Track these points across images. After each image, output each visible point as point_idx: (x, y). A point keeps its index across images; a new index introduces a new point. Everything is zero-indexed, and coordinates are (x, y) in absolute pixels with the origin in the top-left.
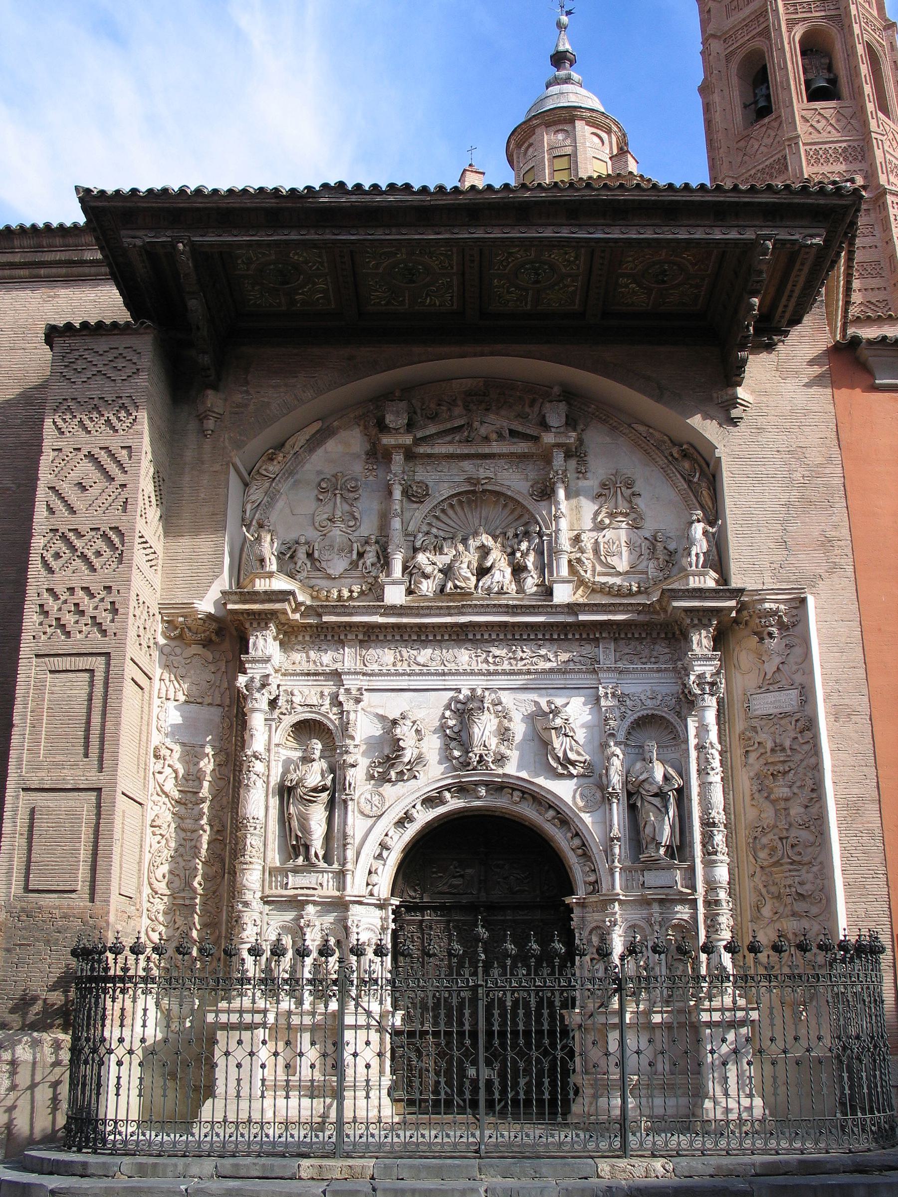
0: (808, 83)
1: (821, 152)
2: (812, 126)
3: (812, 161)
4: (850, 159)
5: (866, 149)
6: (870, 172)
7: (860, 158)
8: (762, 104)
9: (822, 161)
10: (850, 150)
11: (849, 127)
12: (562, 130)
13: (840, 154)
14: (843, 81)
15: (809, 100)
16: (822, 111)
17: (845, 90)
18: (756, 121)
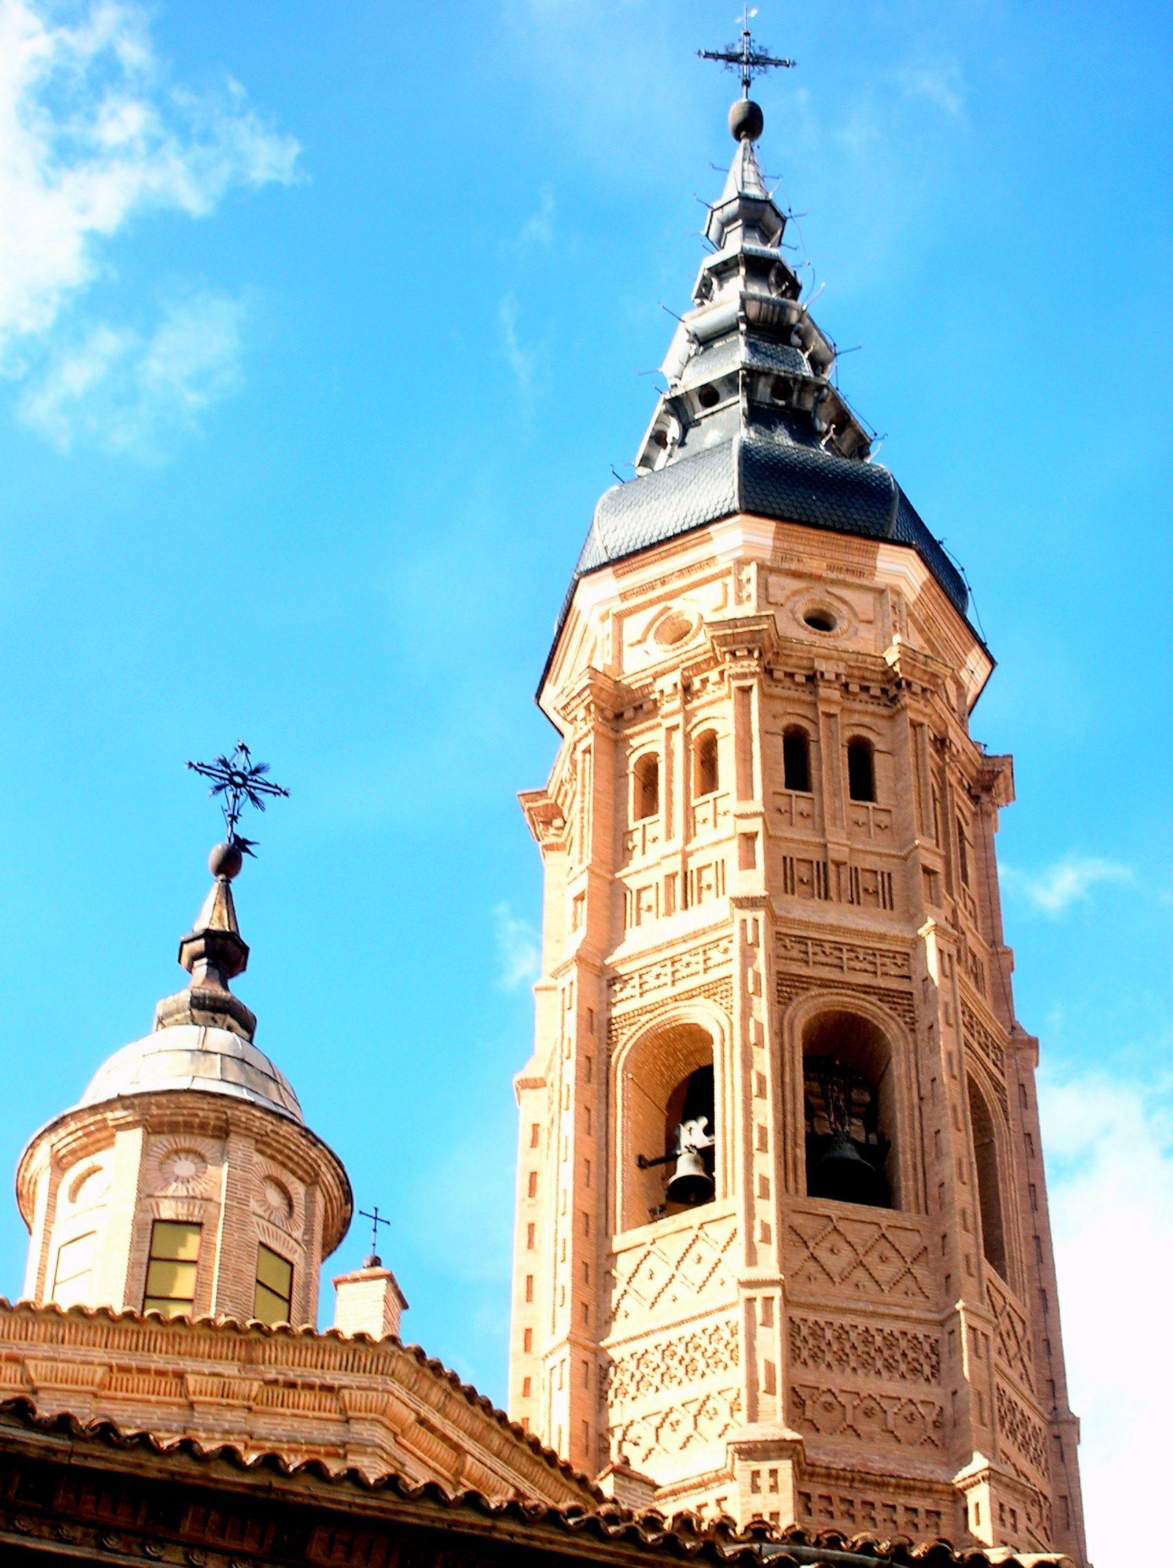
0: (815, 1144)
1: (829, 1334)
2: (813, 1257)
3: (805, 1354)
4: (903, 1367)
5: (944, 1349)
6: (949, 1411)
7: (927, 1370)
8: (685, 1167)
9: (829, 1357)
10: (903, 1343)
11: (908, 1282)
12: (188, 1151)
13: (879, 1350)
14: (905, 1158)
15: (813, 1191)
16: (841, 1226)
17: (907, 1185)
18: (658, 1212)
